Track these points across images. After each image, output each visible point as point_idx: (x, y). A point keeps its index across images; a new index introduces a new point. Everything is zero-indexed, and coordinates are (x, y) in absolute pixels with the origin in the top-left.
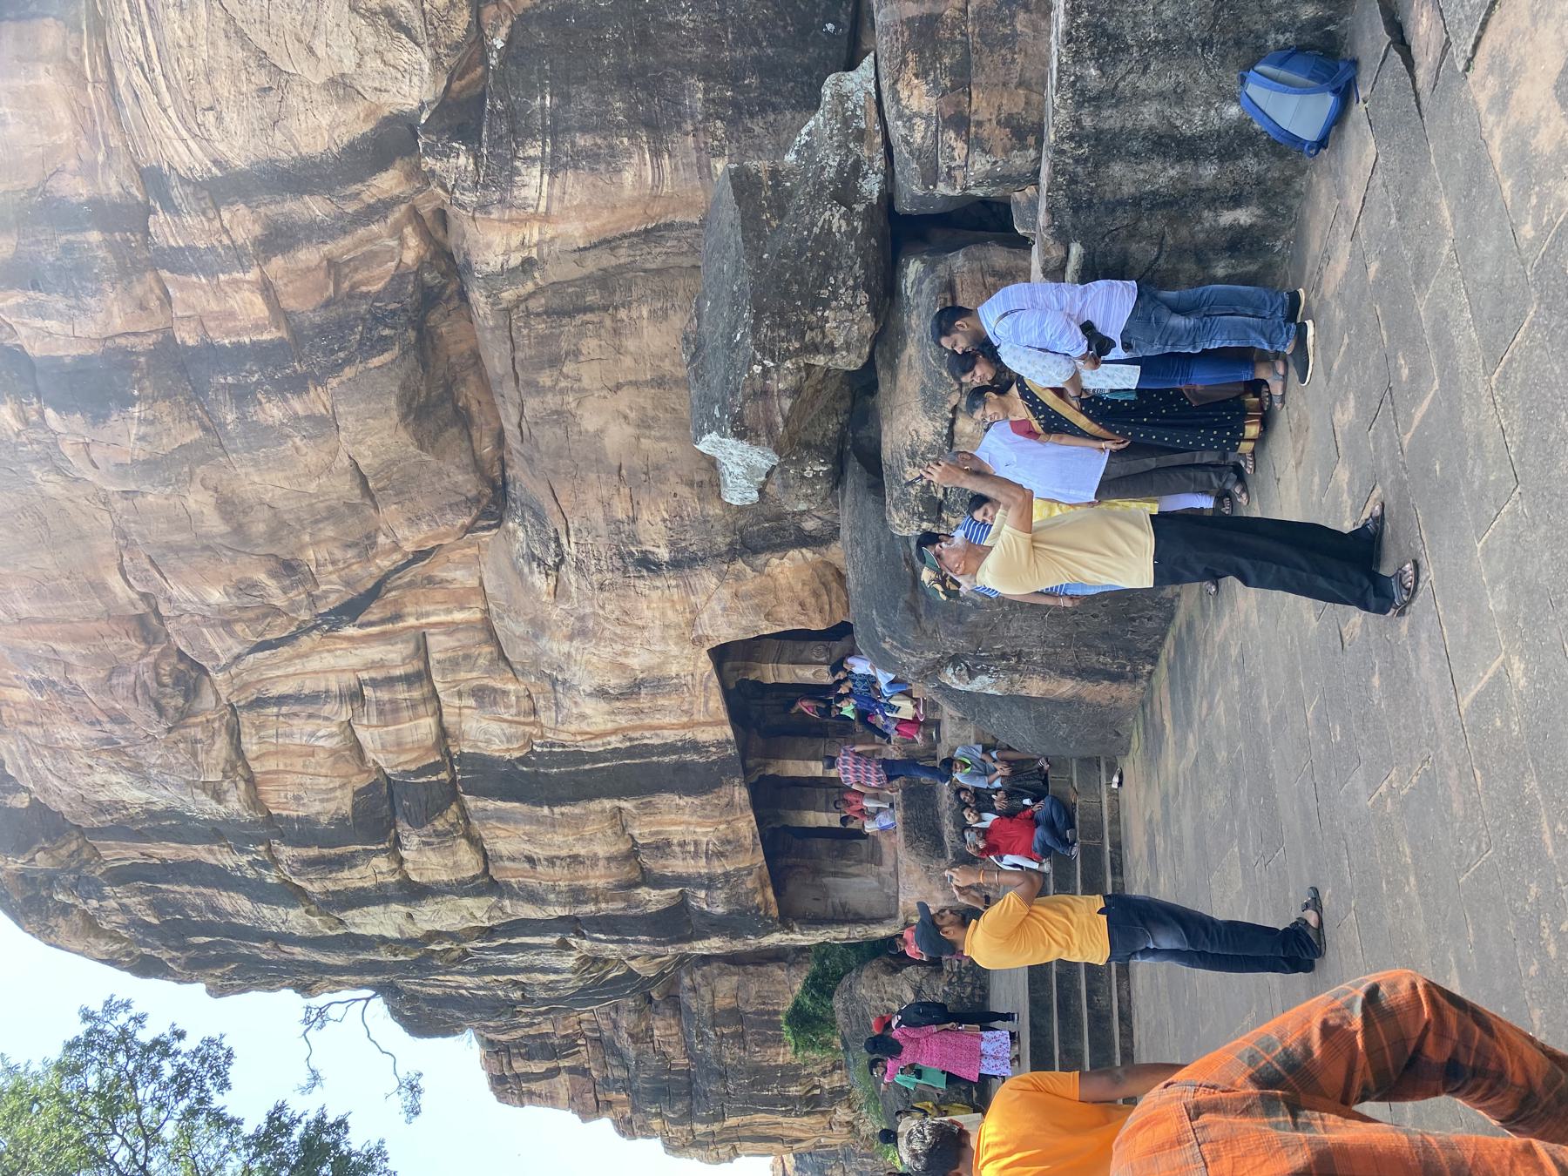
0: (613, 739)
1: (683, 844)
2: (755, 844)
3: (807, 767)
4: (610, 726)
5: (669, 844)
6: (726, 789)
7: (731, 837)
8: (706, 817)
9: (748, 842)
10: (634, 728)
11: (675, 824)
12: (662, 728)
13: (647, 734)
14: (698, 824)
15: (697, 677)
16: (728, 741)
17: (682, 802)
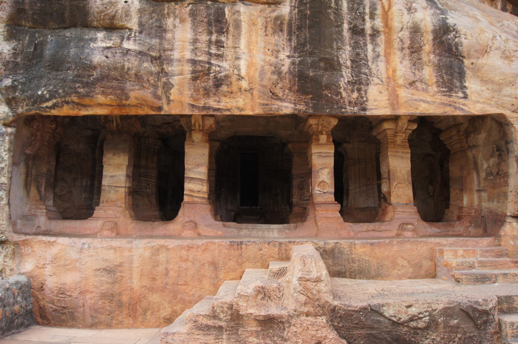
0: (379, 23)
1: (219, 44)
2: (204, 108)
3: (198, 165)
4: (396, 24)
5: (220, 32)
6: (292, 97)
7: (224, 88)
8: (262, 73)
9: (212, 102)
10: (389, 43)
11: (249, 44)
12: (388, 62)
13: (381, 50)
14: (250, 65)
15: (462, 101)
16: (364, 109)
17: (283, 55)
